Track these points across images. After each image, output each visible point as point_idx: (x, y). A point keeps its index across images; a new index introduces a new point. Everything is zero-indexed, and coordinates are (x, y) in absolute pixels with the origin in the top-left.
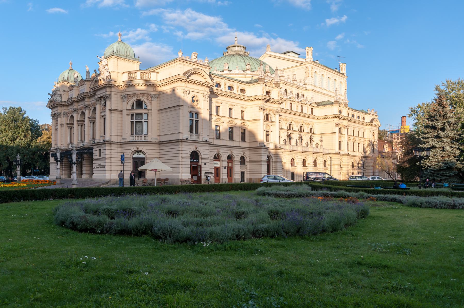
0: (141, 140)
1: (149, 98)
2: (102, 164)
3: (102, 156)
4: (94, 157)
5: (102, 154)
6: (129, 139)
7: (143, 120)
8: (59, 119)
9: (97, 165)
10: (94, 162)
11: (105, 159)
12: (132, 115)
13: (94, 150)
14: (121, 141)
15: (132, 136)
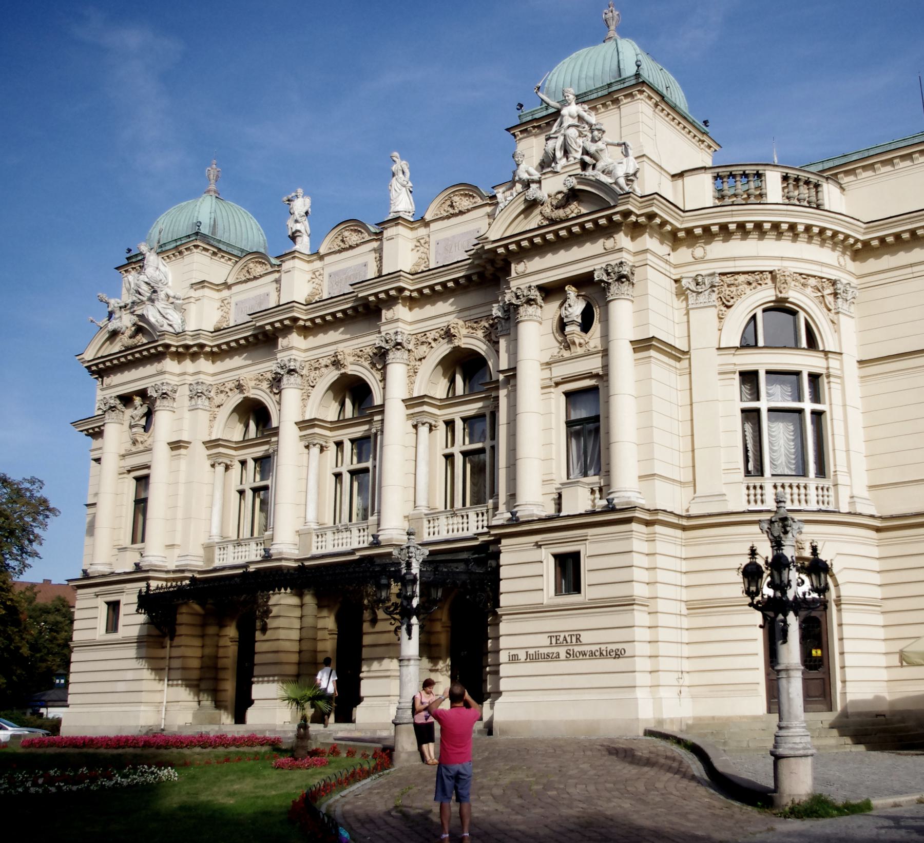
0: (803, 506)
1: (830, 299)
2: (585, 637)
3: (588, 593)
4: (504, 600)
5: (586, 578)
6: (737, 500)
7: (808, 406)
8: (162, 418)
9: (544, 640)
10: (504, 628)
11: (628, 603)
12: (749, 378)
13: (504, 559)
14: (693, 512)
15: (757, 481)
